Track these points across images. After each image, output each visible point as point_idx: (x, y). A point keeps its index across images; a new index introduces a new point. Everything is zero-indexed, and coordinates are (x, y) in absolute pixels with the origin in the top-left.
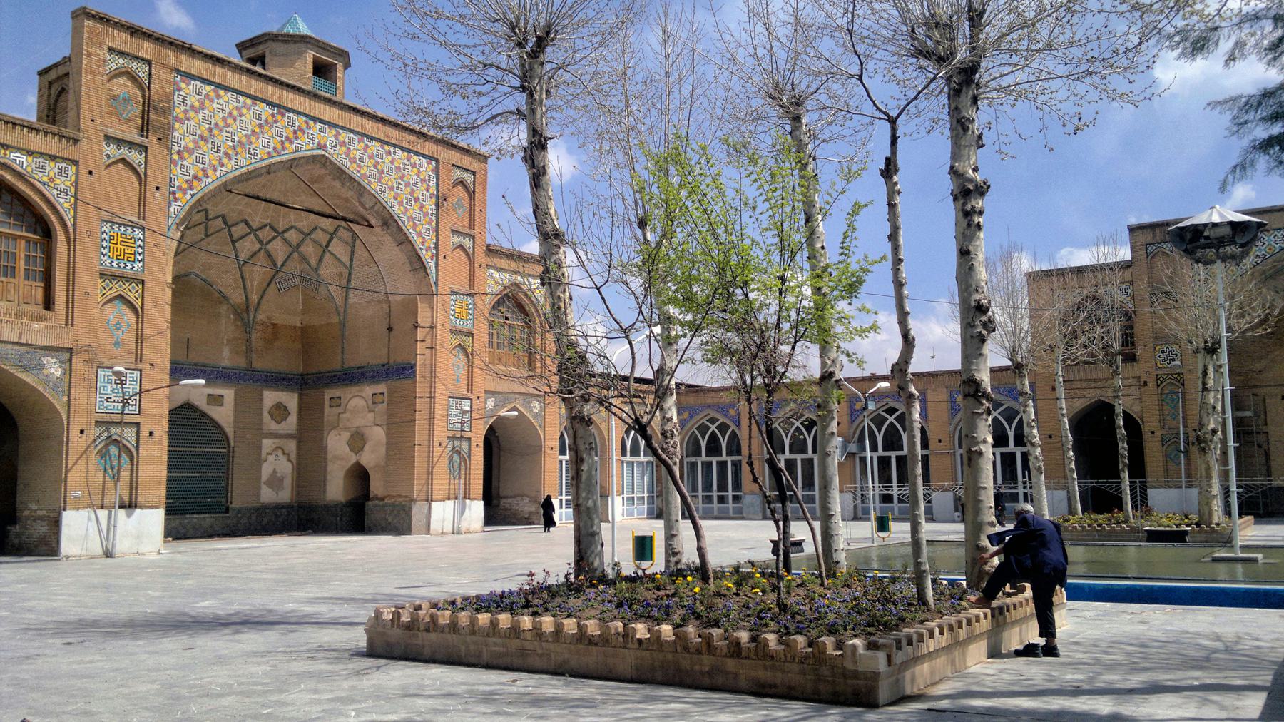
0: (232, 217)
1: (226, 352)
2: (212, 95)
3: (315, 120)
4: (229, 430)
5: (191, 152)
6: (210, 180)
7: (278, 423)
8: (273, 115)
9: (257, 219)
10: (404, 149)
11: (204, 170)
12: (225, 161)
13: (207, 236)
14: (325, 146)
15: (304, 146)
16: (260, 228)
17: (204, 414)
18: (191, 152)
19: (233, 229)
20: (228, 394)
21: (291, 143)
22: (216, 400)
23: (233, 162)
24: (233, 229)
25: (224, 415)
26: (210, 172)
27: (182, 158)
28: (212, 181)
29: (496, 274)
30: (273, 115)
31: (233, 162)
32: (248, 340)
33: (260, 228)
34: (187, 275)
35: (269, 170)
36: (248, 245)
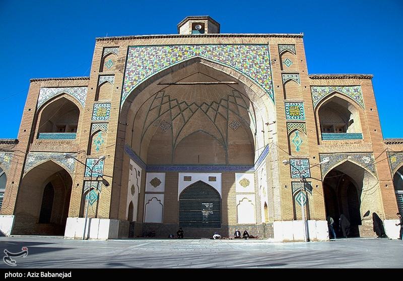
0: (199, 103)
1: (216, 159)
2: (144, 50)
3: (193, 45)
4: (220, 191)
5: (133, 71)
6: (141, 80)
7: (156, 179)
8: (172, 49)
9: (208, 100)
10: (246, 45)
11: (138, 77)
12: (148, 71)
13: (194, 113)
14: (199, 54)
15: (188, 56)
16: (211, 105)
17: (209, 185)
18: (133, 71)
19: (202, 107)
20: (218, 176)
21: (181, 57)
22: (213, 179)
23: (152, 71)
24: (202, 107)
25: (217, 185)
26: (141, 77)
27: (129, 75)
28: (143, 79)
29: (319, 89)
30: (172, 49)
31: (152, 71)
32: (226, 153)
33: (211, 105)
34: (199, 131)
35: (171, 70)
36: (211, 113)
